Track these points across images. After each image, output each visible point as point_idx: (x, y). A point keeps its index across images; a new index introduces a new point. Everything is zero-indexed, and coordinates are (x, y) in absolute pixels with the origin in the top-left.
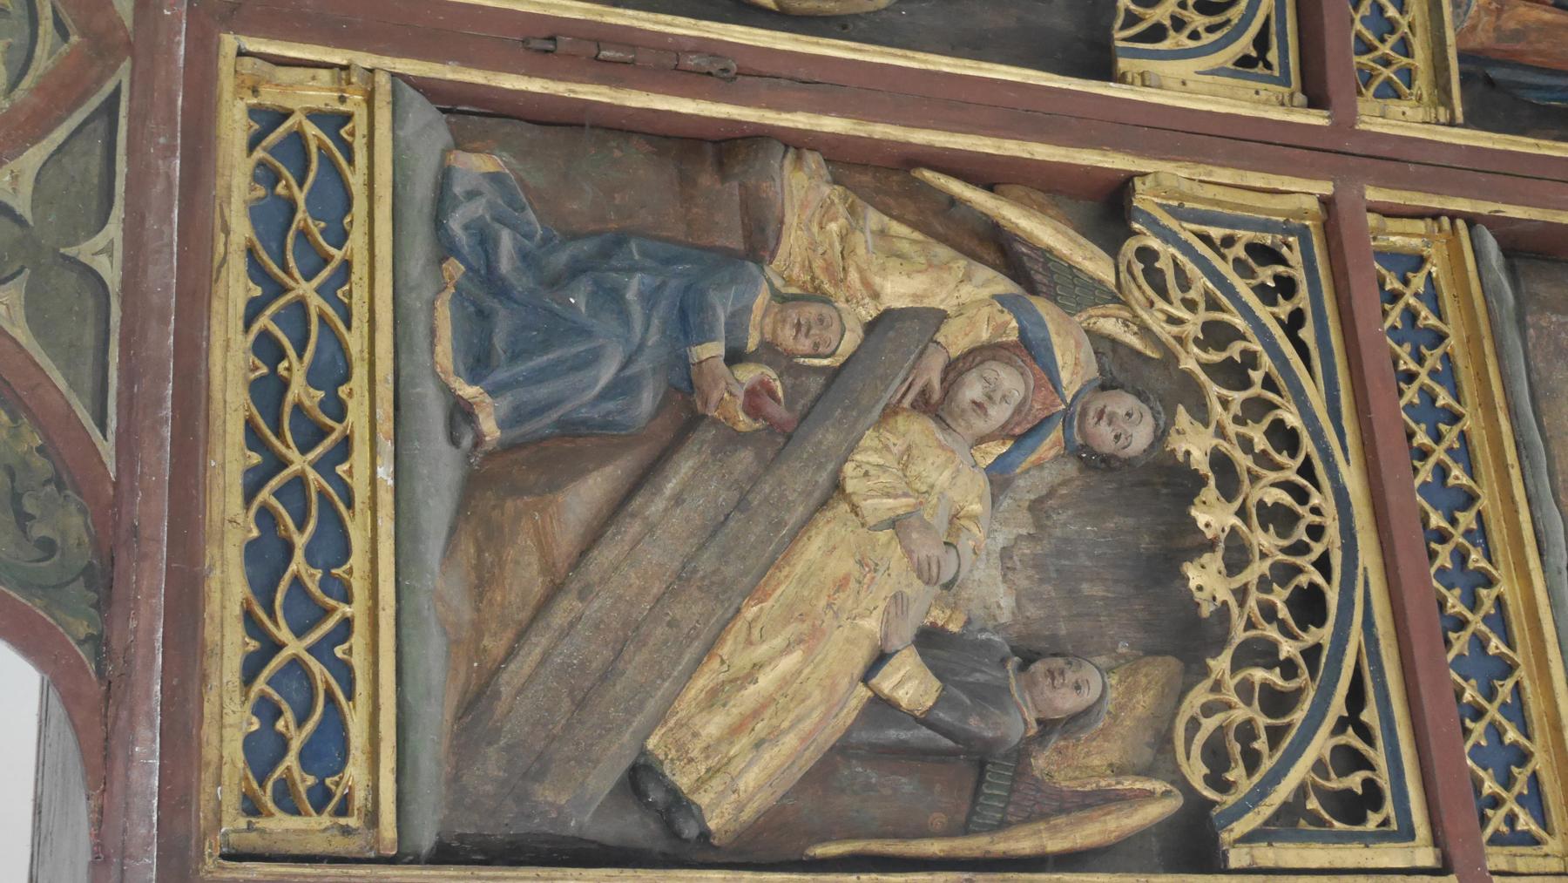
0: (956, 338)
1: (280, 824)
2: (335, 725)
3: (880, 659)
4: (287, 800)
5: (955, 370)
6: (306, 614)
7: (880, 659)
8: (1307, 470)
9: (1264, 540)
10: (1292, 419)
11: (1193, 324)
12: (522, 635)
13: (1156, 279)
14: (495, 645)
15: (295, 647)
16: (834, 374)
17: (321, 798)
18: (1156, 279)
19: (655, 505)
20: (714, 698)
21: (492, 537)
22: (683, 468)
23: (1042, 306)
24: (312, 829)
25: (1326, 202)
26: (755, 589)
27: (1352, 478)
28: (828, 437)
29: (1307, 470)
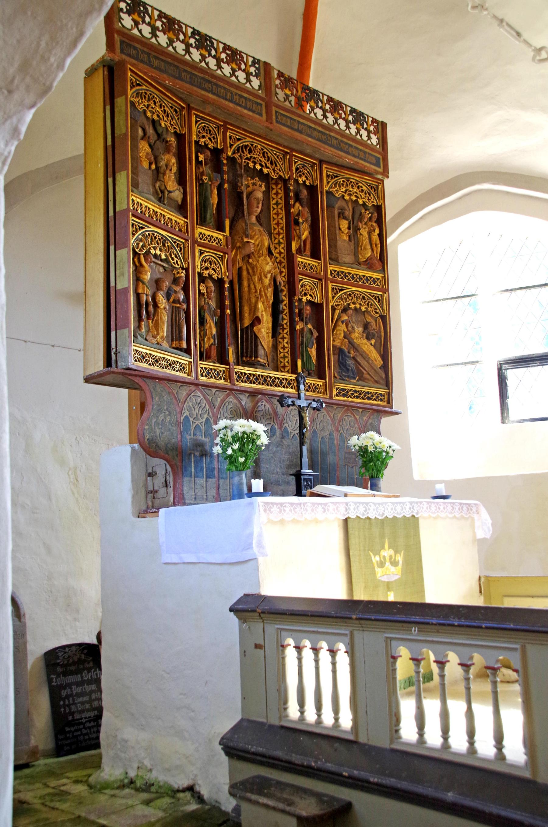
0: (346, 330)
1: (386, 399)
2: (380, 394)
3: (371, 344)
4: (384, 399)
5: (348, 330)
6: (373, 396)
7: (371, 344)
8: (353, 293)
9: (359, 301)
10: (348, 293)
11: (342, 302)
12: (372, 377)
13: (338, 305)
14: (373, 380)
15: (375, 397)
16: (350, 342)
17: (384, 396)
18: (338, 305)
19: (362, 364)
20: (376, 361)
21: (366, 379)
22: (358, 360)
23: (343, 319)
24: (386, 397)
25: (331, 282)
26: (368, 355)
27: (354, 289)
28: (356, 345)
29: (353, 293)
